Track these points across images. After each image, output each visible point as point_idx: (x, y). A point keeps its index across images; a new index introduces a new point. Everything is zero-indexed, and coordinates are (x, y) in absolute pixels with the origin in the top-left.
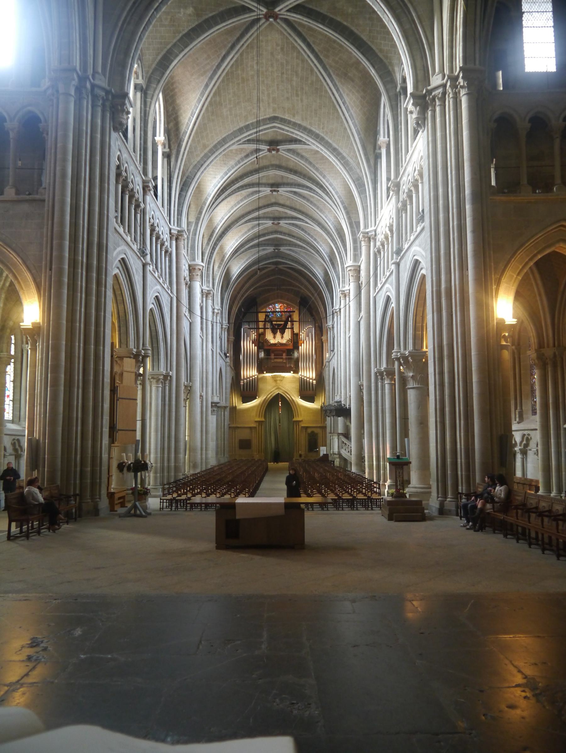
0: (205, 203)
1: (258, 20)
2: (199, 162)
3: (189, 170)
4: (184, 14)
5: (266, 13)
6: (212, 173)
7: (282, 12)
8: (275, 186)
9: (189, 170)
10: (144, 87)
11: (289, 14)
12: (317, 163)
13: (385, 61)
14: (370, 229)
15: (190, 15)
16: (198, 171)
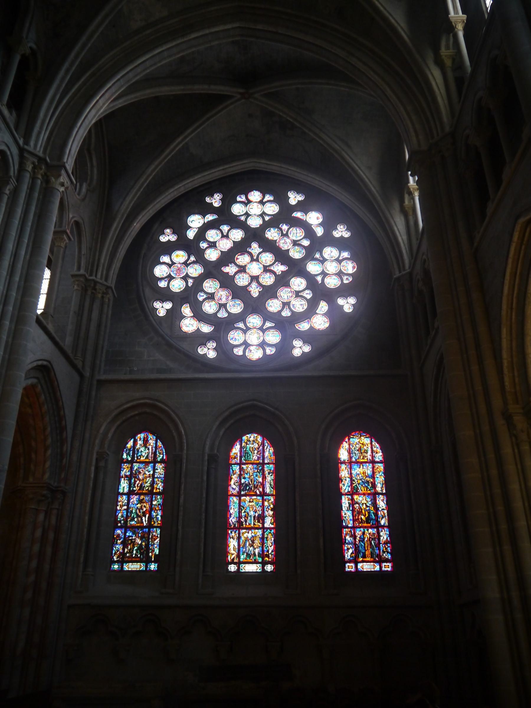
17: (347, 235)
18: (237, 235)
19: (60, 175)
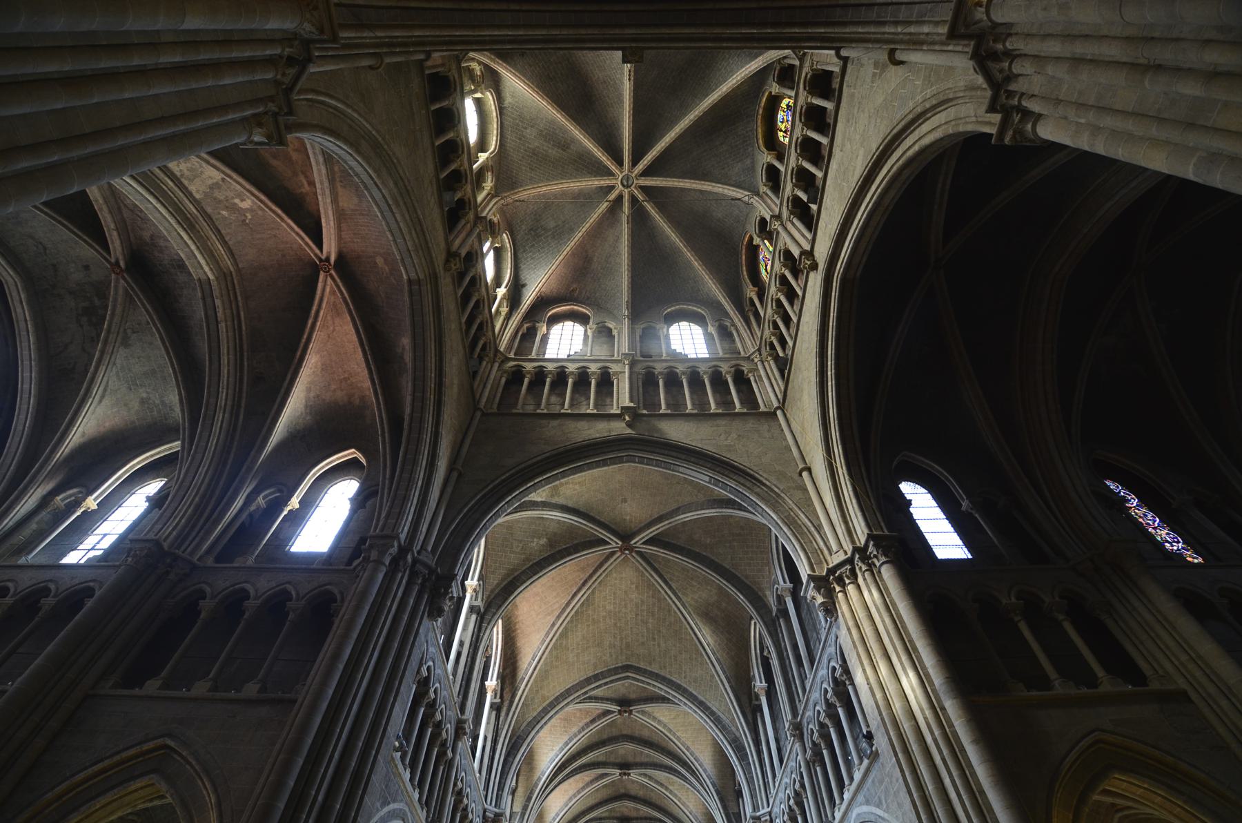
0: (536, 785)
1: (613, 553)
2: (535, 718)
3: (522, 729)
6: (549, 743)
7: (638, 545)
8: (625, 766)
9: (522, 729)
10: (482, 610)
12: (678, 731)
14: (762, 812)
15: (543, 545)
16: (532, 729)
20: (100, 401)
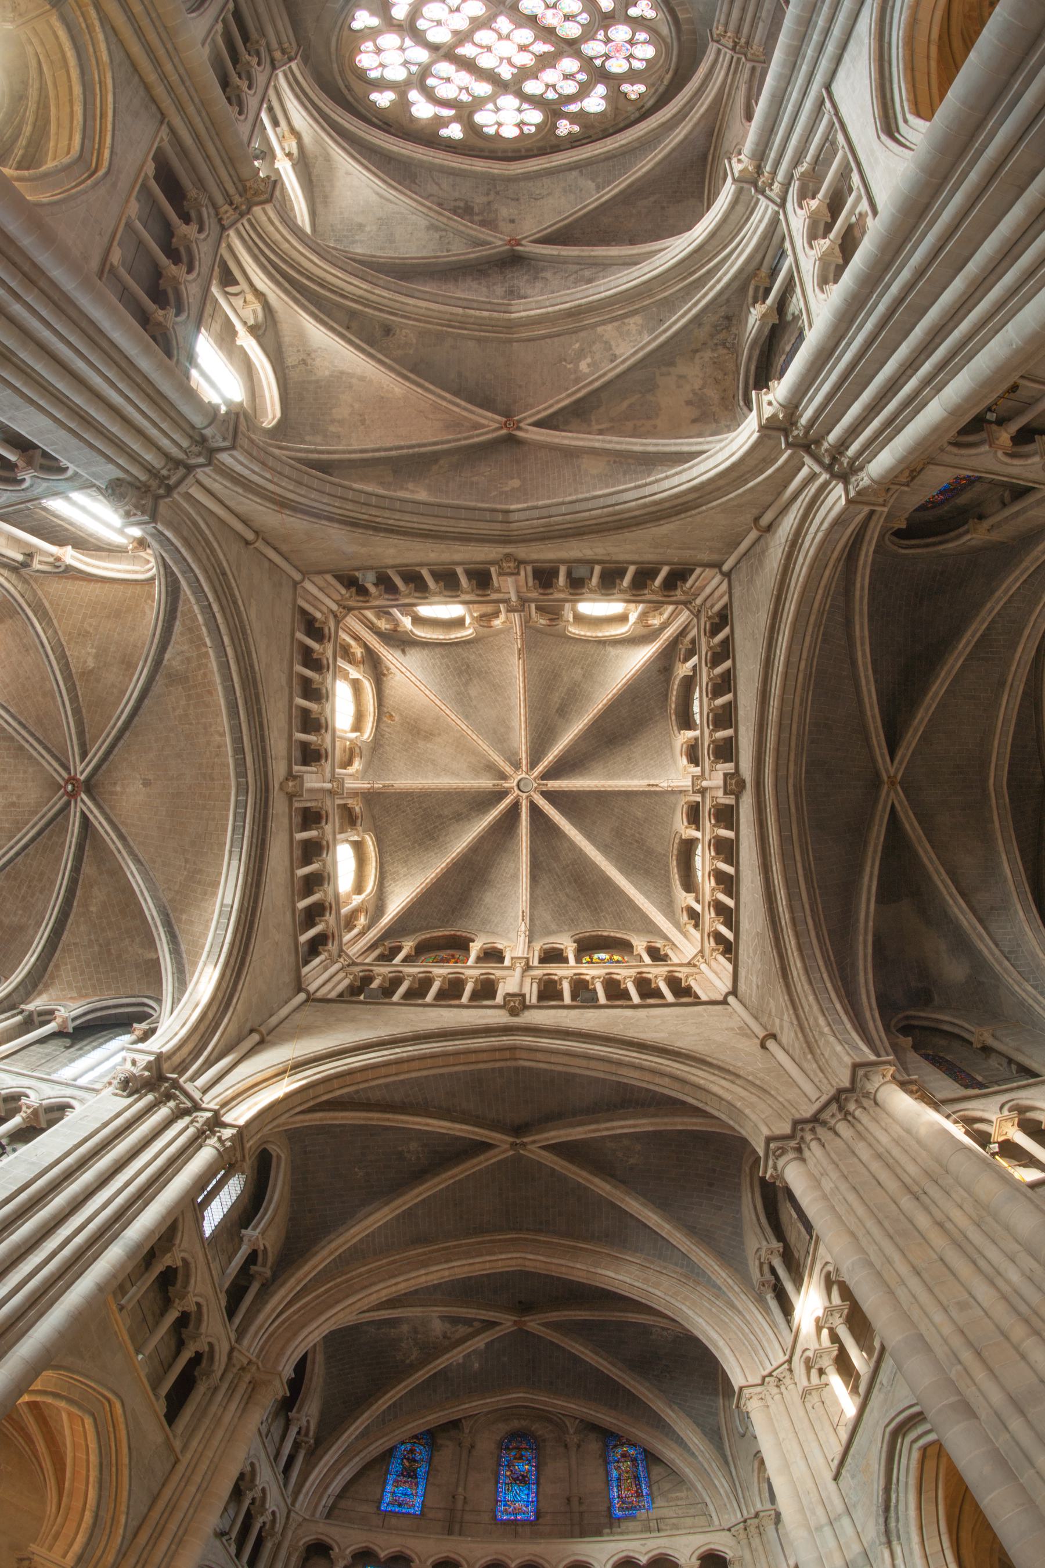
1: (67, 769)
4: (89, 653)
5: (78, 780)
7: (80, 804)
11: (78, 814)
13: (47, 976)
15: (85, 662)
17: (374, 96)
18: (532, 87)
19: (741, 172)
20: (378, 194)
